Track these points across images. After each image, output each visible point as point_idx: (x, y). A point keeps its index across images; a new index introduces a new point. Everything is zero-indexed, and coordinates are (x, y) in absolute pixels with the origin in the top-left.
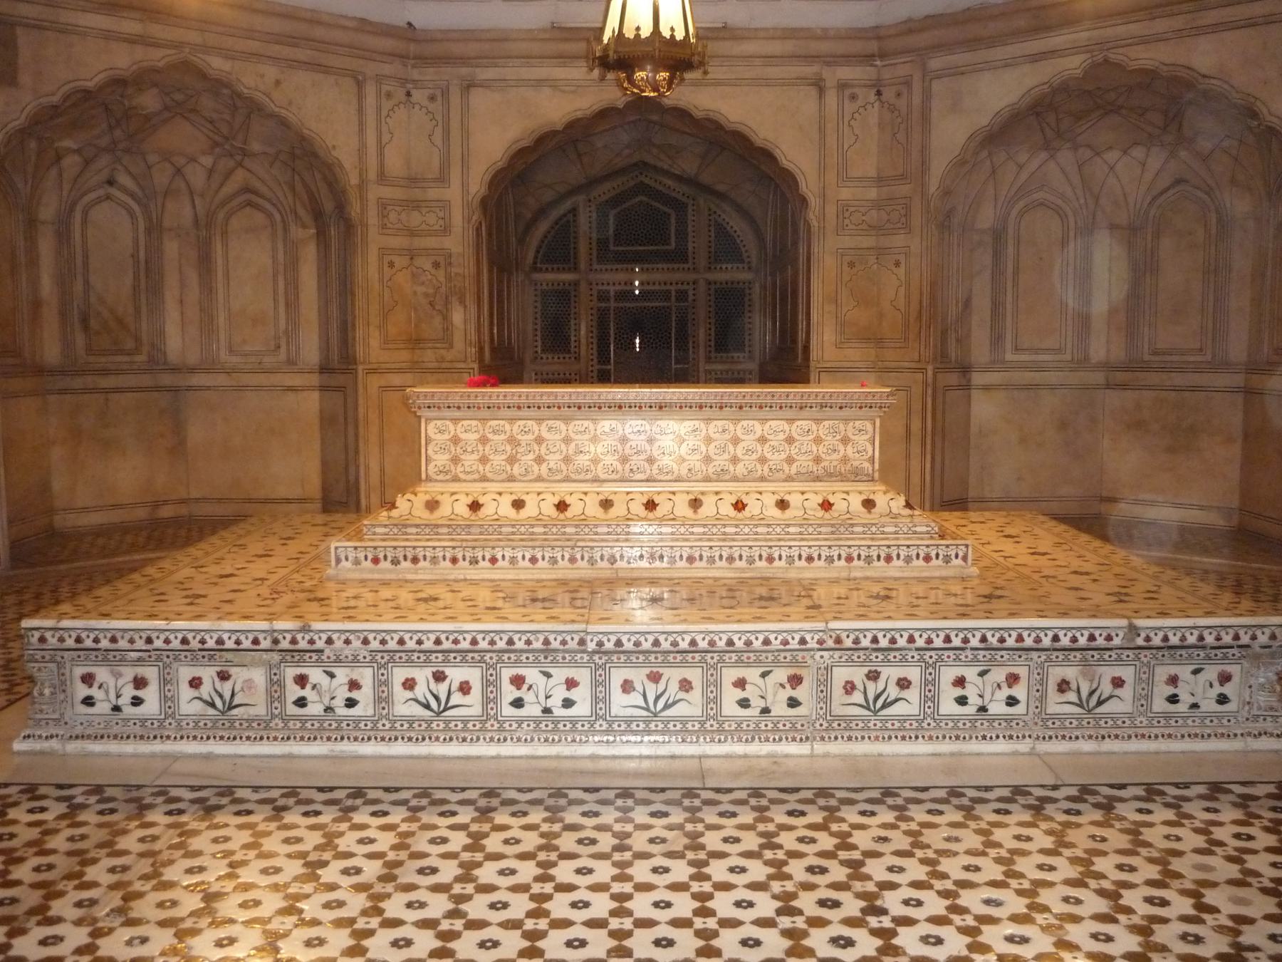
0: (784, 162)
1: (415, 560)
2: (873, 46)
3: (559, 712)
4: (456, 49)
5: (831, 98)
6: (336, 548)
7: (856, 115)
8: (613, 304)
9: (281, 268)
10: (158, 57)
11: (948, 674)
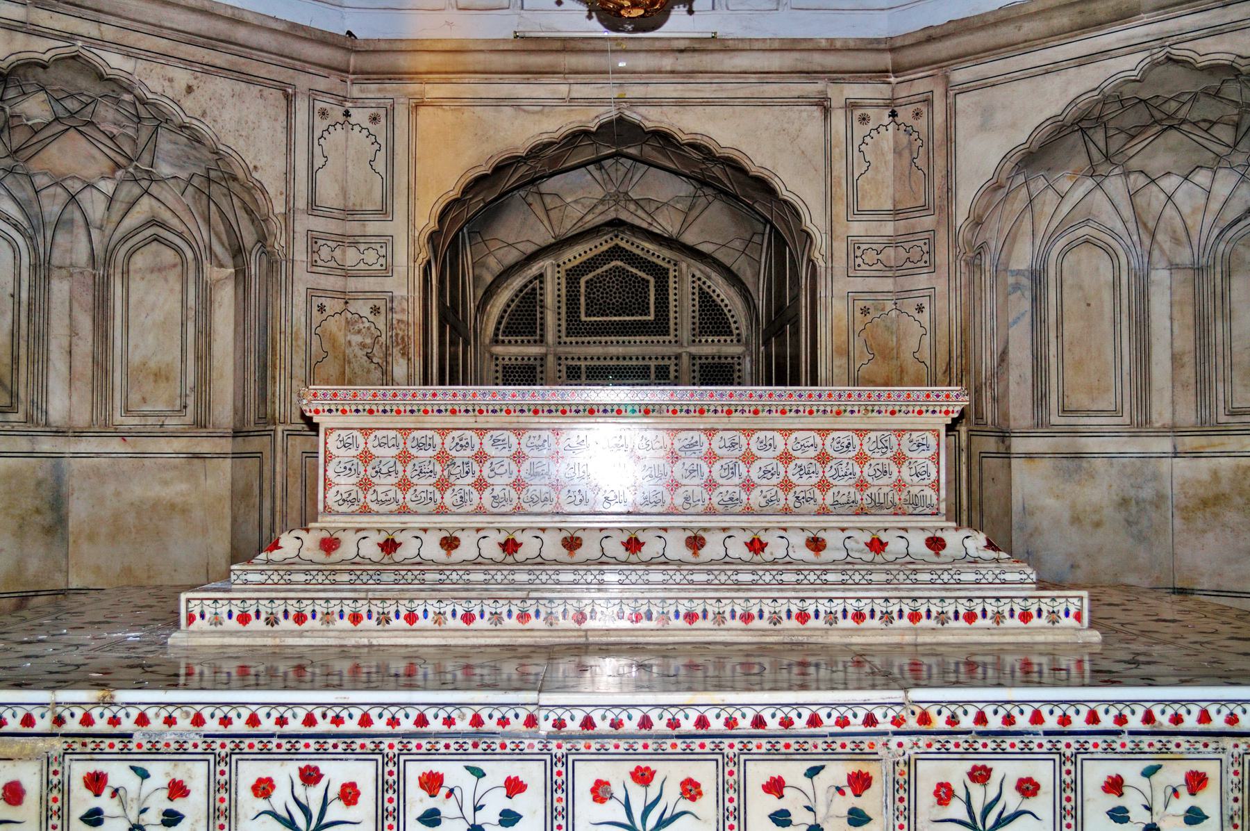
0: (785, 192)
1: (300, 618)
2: (886, 60)
4: (404, 62)
5: (838, 120)
6: (188, 601)
7: (868, 139)
9: (191, 314)
10: (41, 48)
11: (1096, 773)
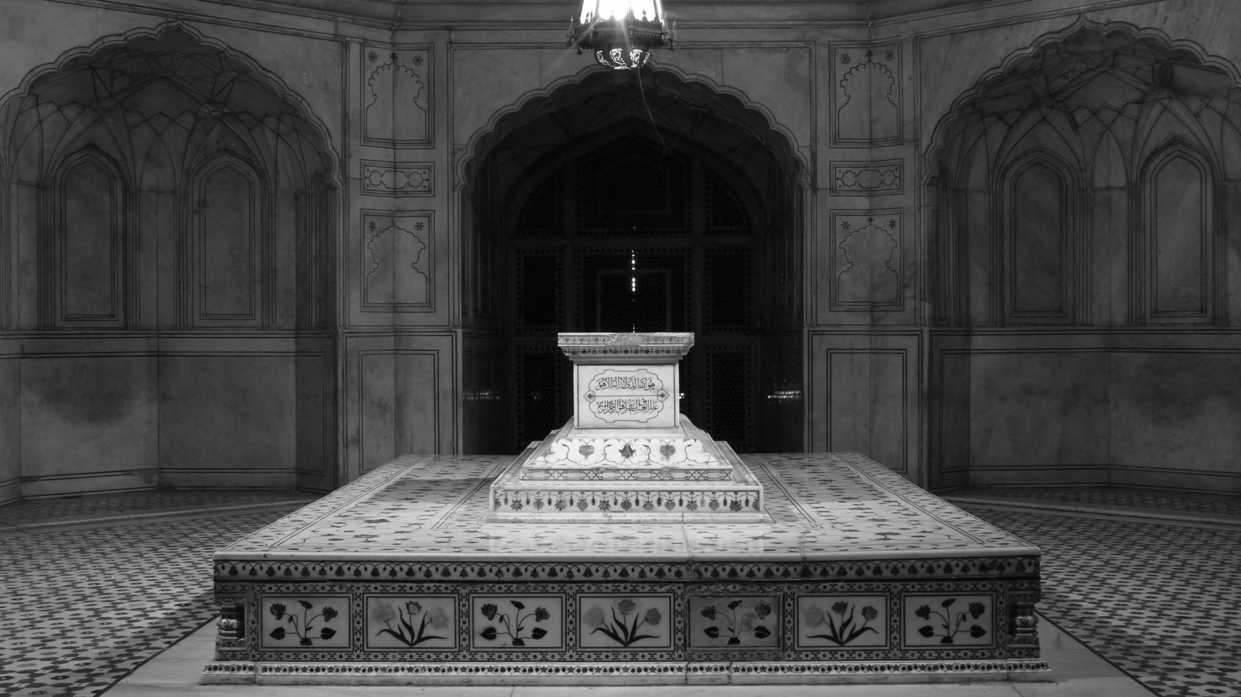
3: (531, 642)
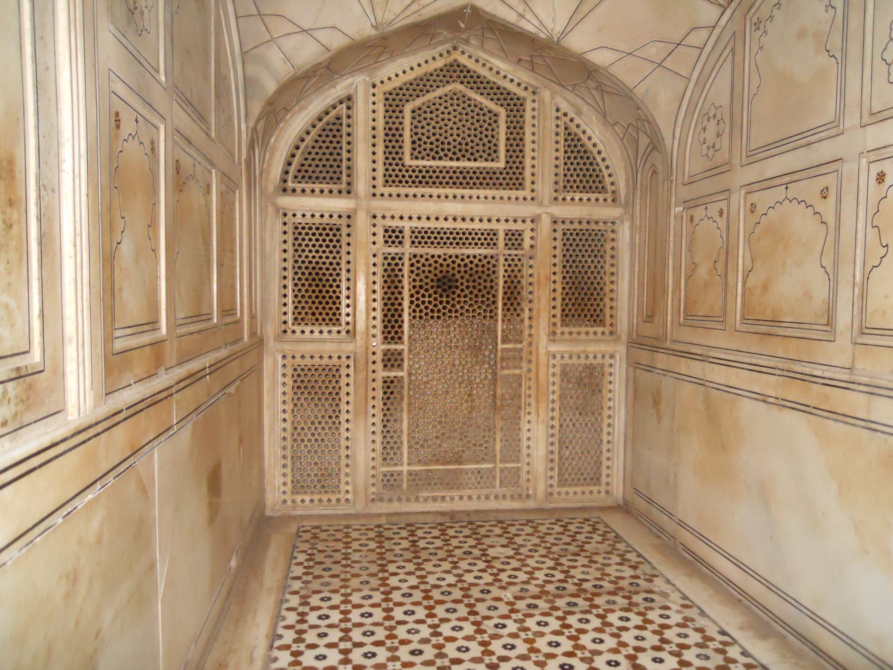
8: (407, 249)
